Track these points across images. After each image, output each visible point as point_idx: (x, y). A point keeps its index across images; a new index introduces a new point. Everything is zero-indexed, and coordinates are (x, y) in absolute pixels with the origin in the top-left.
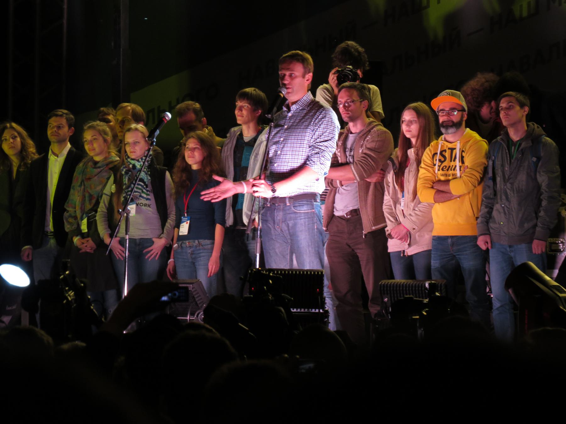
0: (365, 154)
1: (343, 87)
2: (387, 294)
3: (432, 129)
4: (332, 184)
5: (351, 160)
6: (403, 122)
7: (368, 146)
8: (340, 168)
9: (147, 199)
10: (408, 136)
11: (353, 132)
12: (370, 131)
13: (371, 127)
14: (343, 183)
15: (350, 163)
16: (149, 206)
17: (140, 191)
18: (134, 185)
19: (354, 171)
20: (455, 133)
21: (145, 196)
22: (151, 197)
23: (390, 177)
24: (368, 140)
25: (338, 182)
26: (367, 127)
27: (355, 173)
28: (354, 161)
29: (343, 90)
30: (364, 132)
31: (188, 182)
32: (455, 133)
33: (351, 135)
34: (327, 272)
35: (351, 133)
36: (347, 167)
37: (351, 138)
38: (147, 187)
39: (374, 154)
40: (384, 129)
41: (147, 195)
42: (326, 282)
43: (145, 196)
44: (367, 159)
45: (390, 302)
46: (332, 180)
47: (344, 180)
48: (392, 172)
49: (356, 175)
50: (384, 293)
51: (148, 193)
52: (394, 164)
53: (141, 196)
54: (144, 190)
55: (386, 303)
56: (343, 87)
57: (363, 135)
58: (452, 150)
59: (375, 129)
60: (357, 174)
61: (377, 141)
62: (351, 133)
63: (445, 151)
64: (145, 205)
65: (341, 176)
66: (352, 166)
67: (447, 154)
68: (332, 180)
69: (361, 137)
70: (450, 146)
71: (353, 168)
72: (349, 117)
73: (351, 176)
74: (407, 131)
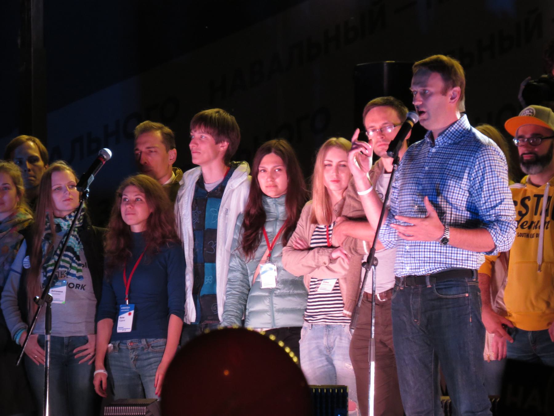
9: (79, 278)
16: (83, 287)
17: (68, 265)
18: (60, 256)
21: (74, 272)
22: (86, 273)
31: (127, 251)
38: (78, 258)
41: (78, 271)
43: (74, 272)
51: (81, 268)
53: (68, 273)
54: (74, 265)
58: (539, 197)
63: (529, 198)
64: (78, 286)
70: (536, 191)
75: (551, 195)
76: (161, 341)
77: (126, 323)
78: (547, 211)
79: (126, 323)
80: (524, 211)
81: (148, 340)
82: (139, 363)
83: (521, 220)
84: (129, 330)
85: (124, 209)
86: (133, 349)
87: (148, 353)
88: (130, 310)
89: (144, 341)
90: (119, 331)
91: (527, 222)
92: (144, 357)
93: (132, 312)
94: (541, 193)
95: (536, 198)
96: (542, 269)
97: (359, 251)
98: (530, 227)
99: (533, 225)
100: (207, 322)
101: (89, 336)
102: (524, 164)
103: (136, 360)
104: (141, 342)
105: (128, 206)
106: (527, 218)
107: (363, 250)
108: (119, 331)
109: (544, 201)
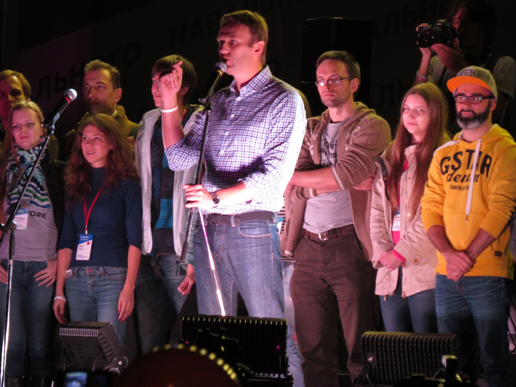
0: (352, 152)
1: (326, 57)
2: (373, 351)
3: (447, 120)
4: (303, 195)
5: (332, 160)
6: (404, 109)
7: (357, 141)
8: (315, 172)
10: (411, 130)
11: (334, 120)
12: (358, 120)
13: (360, 114)
14: (318, 192)
15: (330, 164)
19: (336, 175)
20: (477, 128)
23: (380, 186)
24: (356, 134)
25: (311, 191)
26: (355, 114)
27: (338, 178)
28: (336, 161)
29: (326, 61)
30: (352, 120)
32: (477, 128)
33: (330, 125)
34: (290, 317)
35: (332, 122)
36: (326, 171)
37: (331, 128)
39: (365, 152)
40: (380, 118)
42: (291, 332)
44: (355, 159)
45: (376, 362)
46: (303, 189)
47: (320, 189)
48: (381, 180)
49: (339, 181)
50: (368, 351)
52: (384, 168)
55: (370, 364)
56: (326, 57)
57: (349, 126)
59: (365, 117)
60: (341, 179)
61: (370, 134)
62: (332, 122)
65: (318, 183)
66: (333, 168)
67: (463, 158)
68: (303, 189)
69: (346, 128)
71: (334, 171)
72: (333, 101)
73: (333, 183)
74: (410, 124)
75: (482, 151)
76: (118, 270)
77: (84, 251)
78: (477, 165)
79: (84, 251)
80: (457, 165)
81: (106, 268)
82: (95, 288)
83: (454, 173)
84: (87, 259)
85: (85, 147)
86: (91, 276)
87: (105, 280)
88: (89, 239)
89: (101, 269)
90: (78, 258)
91: (460, 176)
92: (101, 283)
93: (91, 242)
94: (472, 149)
95: (468, 153)
96: (470, 218)
97: (305, 195)
98: (462, 181)
99: (466, 178)
100: (161, 253)
101: (48, 262)
102: (462, 120)
103: (94, 285)
104: (98, 269)
105: (88, 145)
106: (459, 172)
107: (309, 194)
108: (78, 258)
109: (475, 155)
